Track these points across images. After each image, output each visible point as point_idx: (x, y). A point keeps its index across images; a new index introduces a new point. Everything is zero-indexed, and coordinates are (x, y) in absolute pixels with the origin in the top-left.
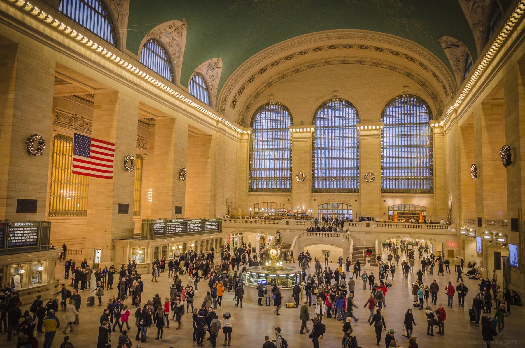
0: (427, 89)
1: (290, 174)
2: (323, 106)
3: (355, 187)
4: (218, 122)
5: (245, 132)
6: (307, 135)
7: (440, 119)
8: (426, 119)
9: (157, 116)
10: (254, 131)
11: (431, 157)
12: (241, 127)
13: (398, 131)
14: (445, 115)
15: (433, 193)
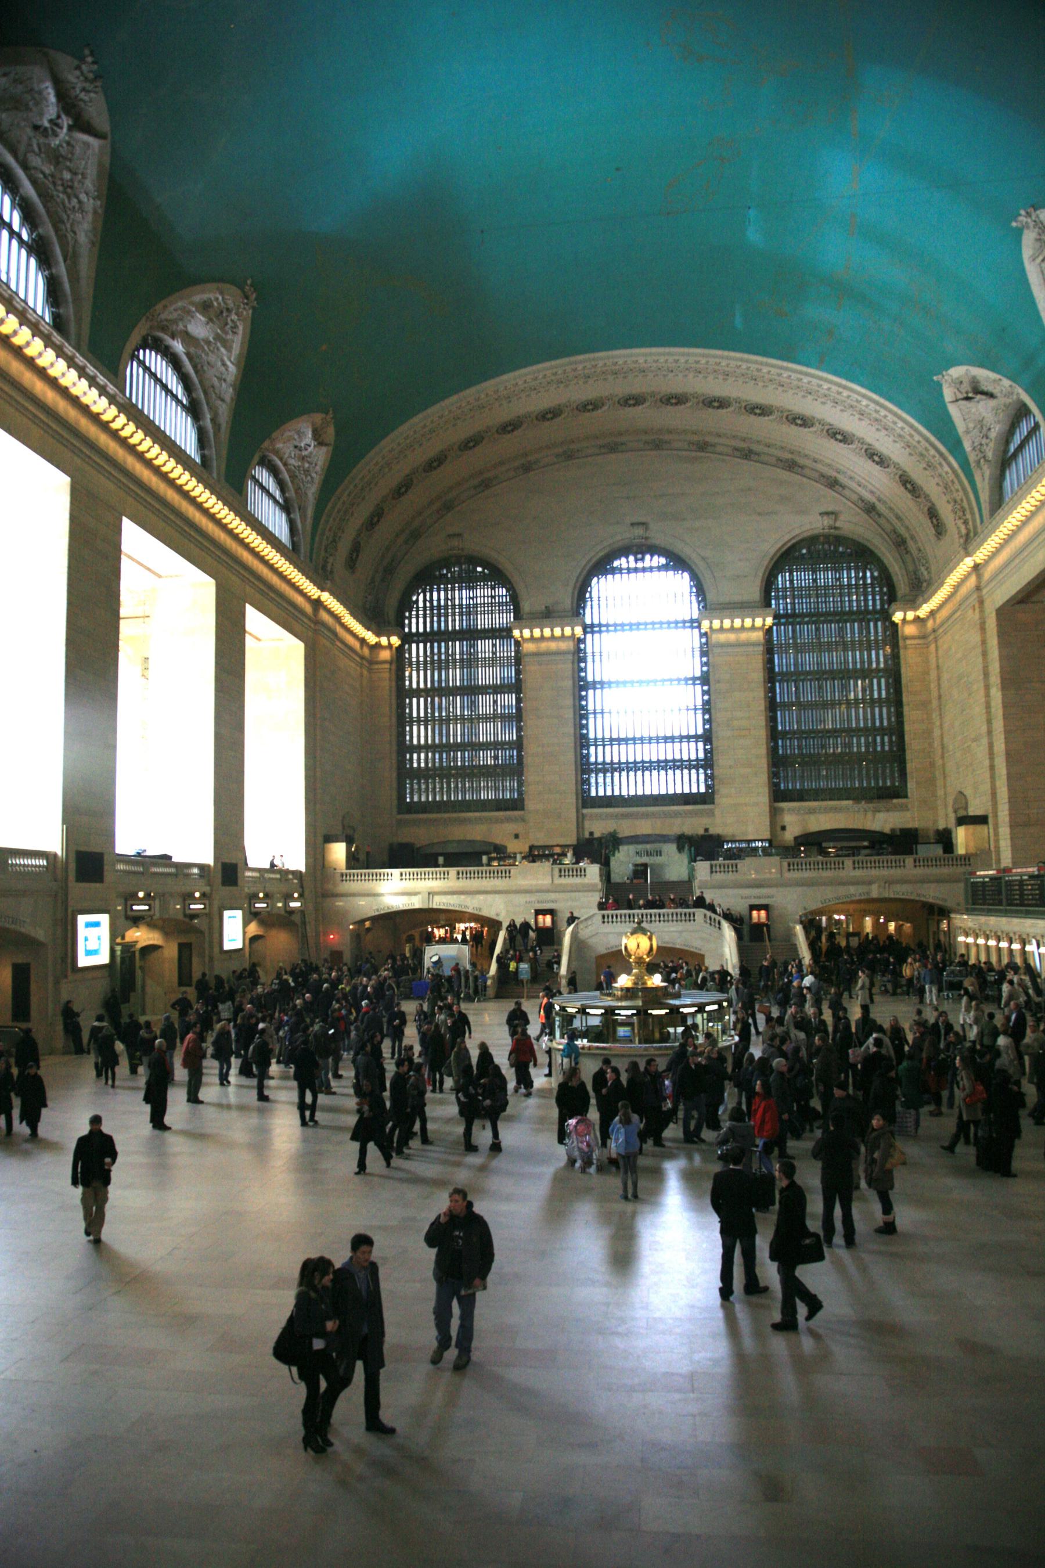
0: (882, 521)
1: (520, 757)
2: (603, 566)
3: (702, 790)
4: (317, 604)
5: (384, 641)
6: (563, 646)
7: (921, 599)
8: (874, 602)
9: (160, 576)
10: (408, 639)
11: (896, 700)
12: (373, 626)
13: (806, 632)
14: (942, 584)
15: (906, 797)
